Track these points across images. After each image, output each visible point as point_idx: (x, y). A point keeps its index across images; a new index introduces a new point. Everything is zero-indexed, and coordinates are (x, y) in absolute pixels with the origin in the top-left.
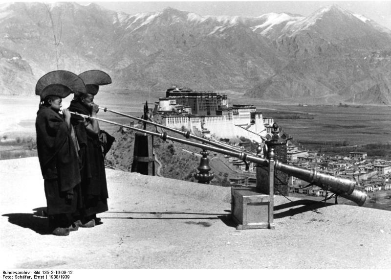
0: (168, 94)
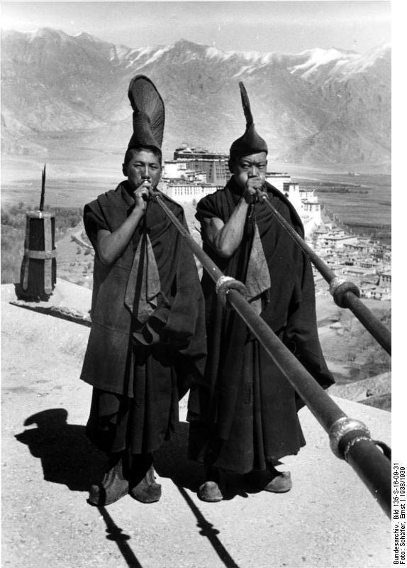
0: (176, 156)
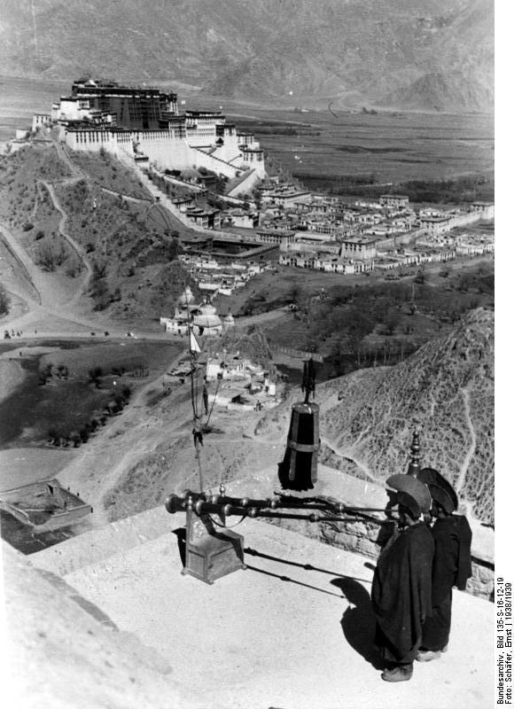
0: (76, 90)
